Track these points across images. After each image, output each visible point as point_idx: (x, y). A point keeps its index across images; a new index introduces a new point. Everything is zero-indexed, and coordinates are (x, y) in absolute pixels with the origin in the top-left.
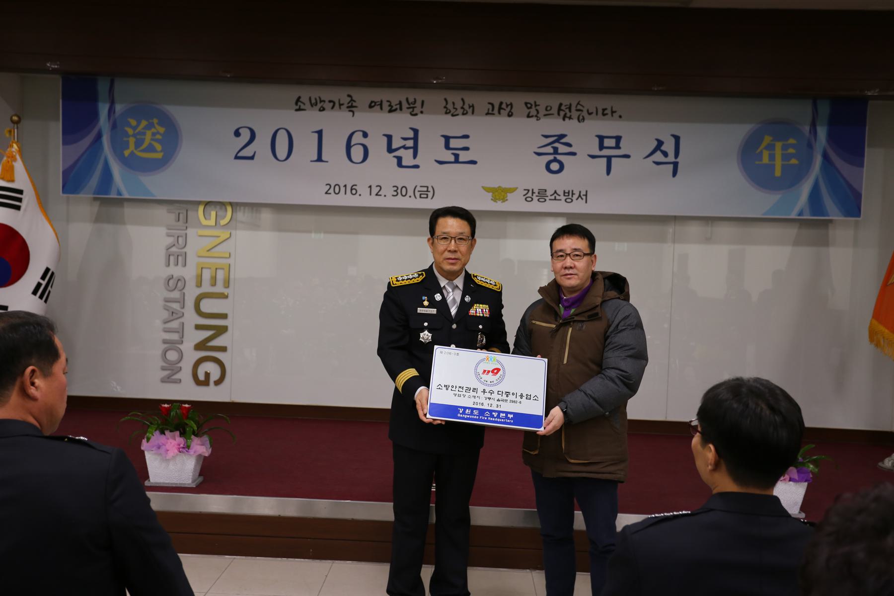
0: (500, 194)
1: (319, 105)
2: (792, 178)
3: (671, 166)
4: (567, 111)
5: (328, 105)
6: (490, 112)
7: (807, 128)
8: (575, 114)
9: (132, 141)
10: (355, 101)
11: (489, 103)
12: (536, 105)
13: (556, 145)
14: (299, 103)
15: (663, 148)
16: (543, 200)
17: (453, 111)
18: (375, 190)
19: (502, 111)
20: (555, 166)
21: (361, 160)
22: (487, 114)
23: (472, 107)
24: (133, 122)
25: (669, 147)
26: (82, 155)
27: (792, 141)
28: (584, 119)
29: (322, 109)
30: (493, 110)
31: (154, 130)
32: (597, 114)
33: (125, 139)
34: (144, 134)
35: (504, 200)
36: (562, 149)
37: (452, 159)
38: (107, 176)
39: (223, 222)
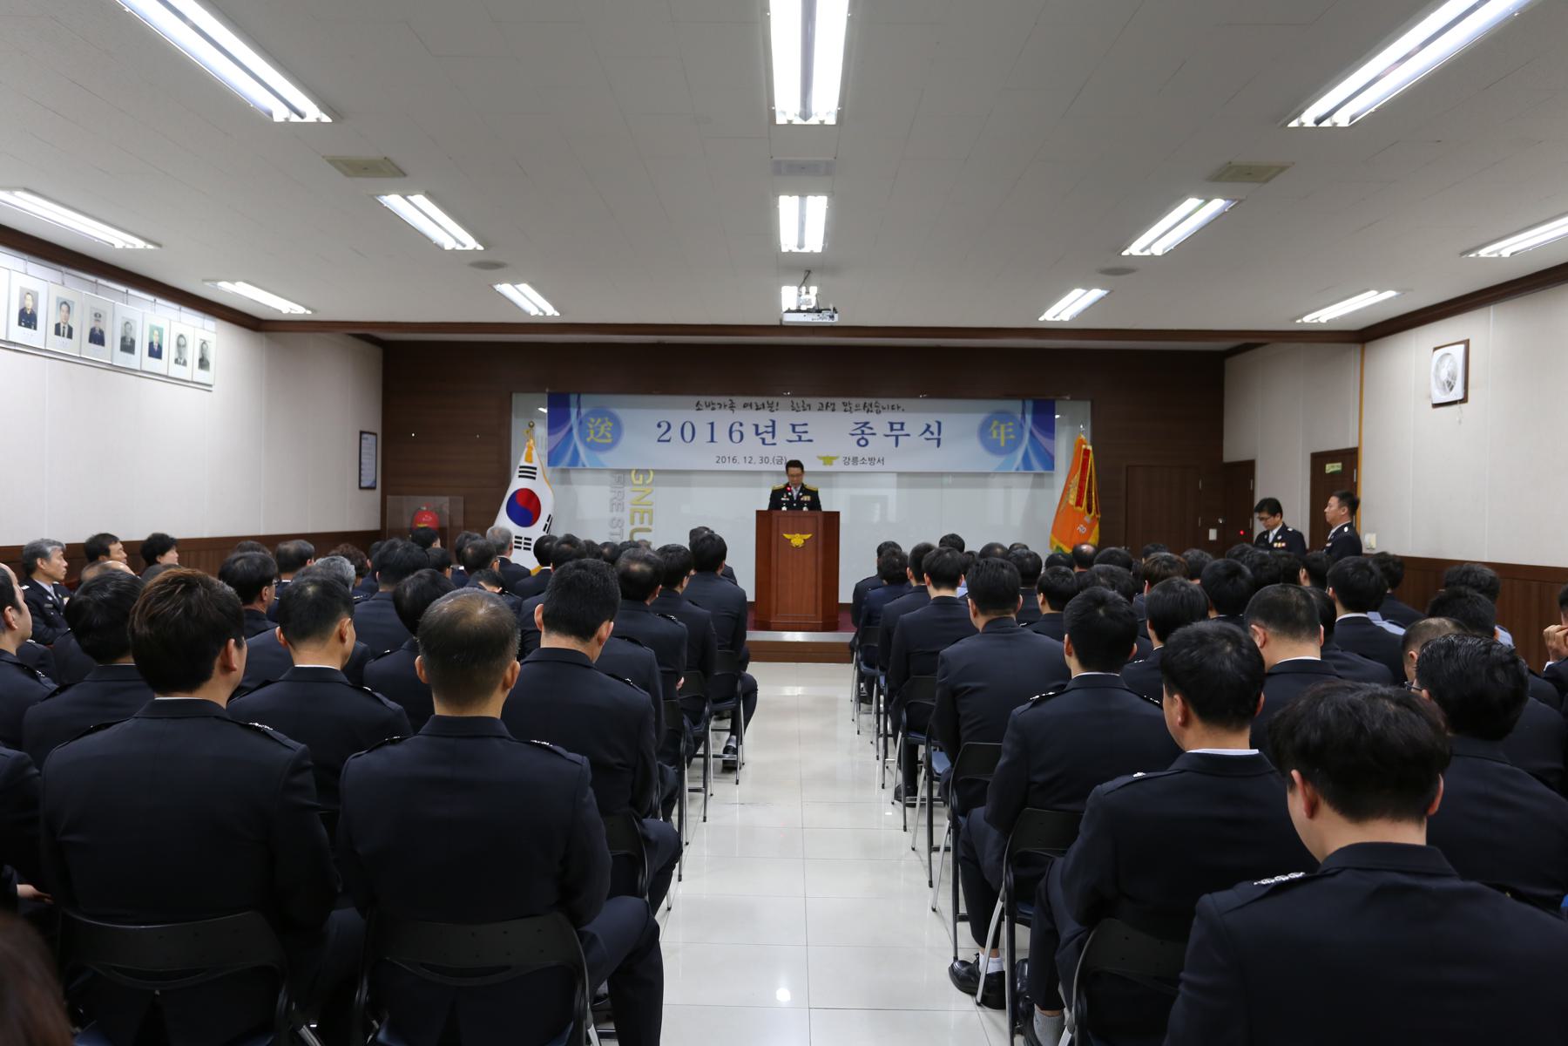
0: (828, 460)
2: (1011, 447)
3: (936, 441)
7: (1019, 416)
9: (592, 432)
13: (863, 429)
15: (931, 429)
18: (748, 460)
20: (863, 442)
22: (819, 410)
23: (809, 406)
24: (593, 420)
25: (934, 428)
27: (1011, 424)
29: (713, 409)
35: (831, 464)
36: (867, 431)
37: (797, 438)
38: (576, 454)
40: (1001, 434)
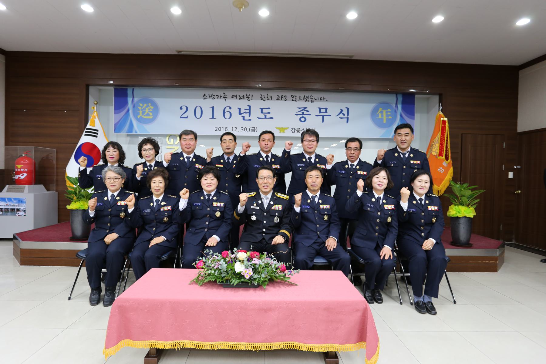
1: (212, 97)
2: (390, 123)
3: (346, 119)
4: (307, 98)
5: (216, 97)
6: (278, 99)
7: (394, 105)
8: (310, 100)
9: (141, 112)
10: (226, 95)
11: (278, 96)
12: (295, 96)
13: (303, 111)
14: (205, 96)
15: (343, 112)
16: (299, 132)
17: (264, 99)
19: (282, 98)
20: (303, 119)
21: (229, 117)
22: (277, 100)
23: (271, 97)
24: (141, 105)
25: (345, 112)
26: (122, 118)
27: (389, 110)
28: (313, 101)
29: (214, 99)
30: (279, 98)
31: (149, 108)
32: (318, 100)
33: (138, 111)
34: (145, 109)
35: (284, 132)
36: (305, 113)
37: (264, 117)
38: (131, 125)
39: (176, 143)
40: (384, 115)
